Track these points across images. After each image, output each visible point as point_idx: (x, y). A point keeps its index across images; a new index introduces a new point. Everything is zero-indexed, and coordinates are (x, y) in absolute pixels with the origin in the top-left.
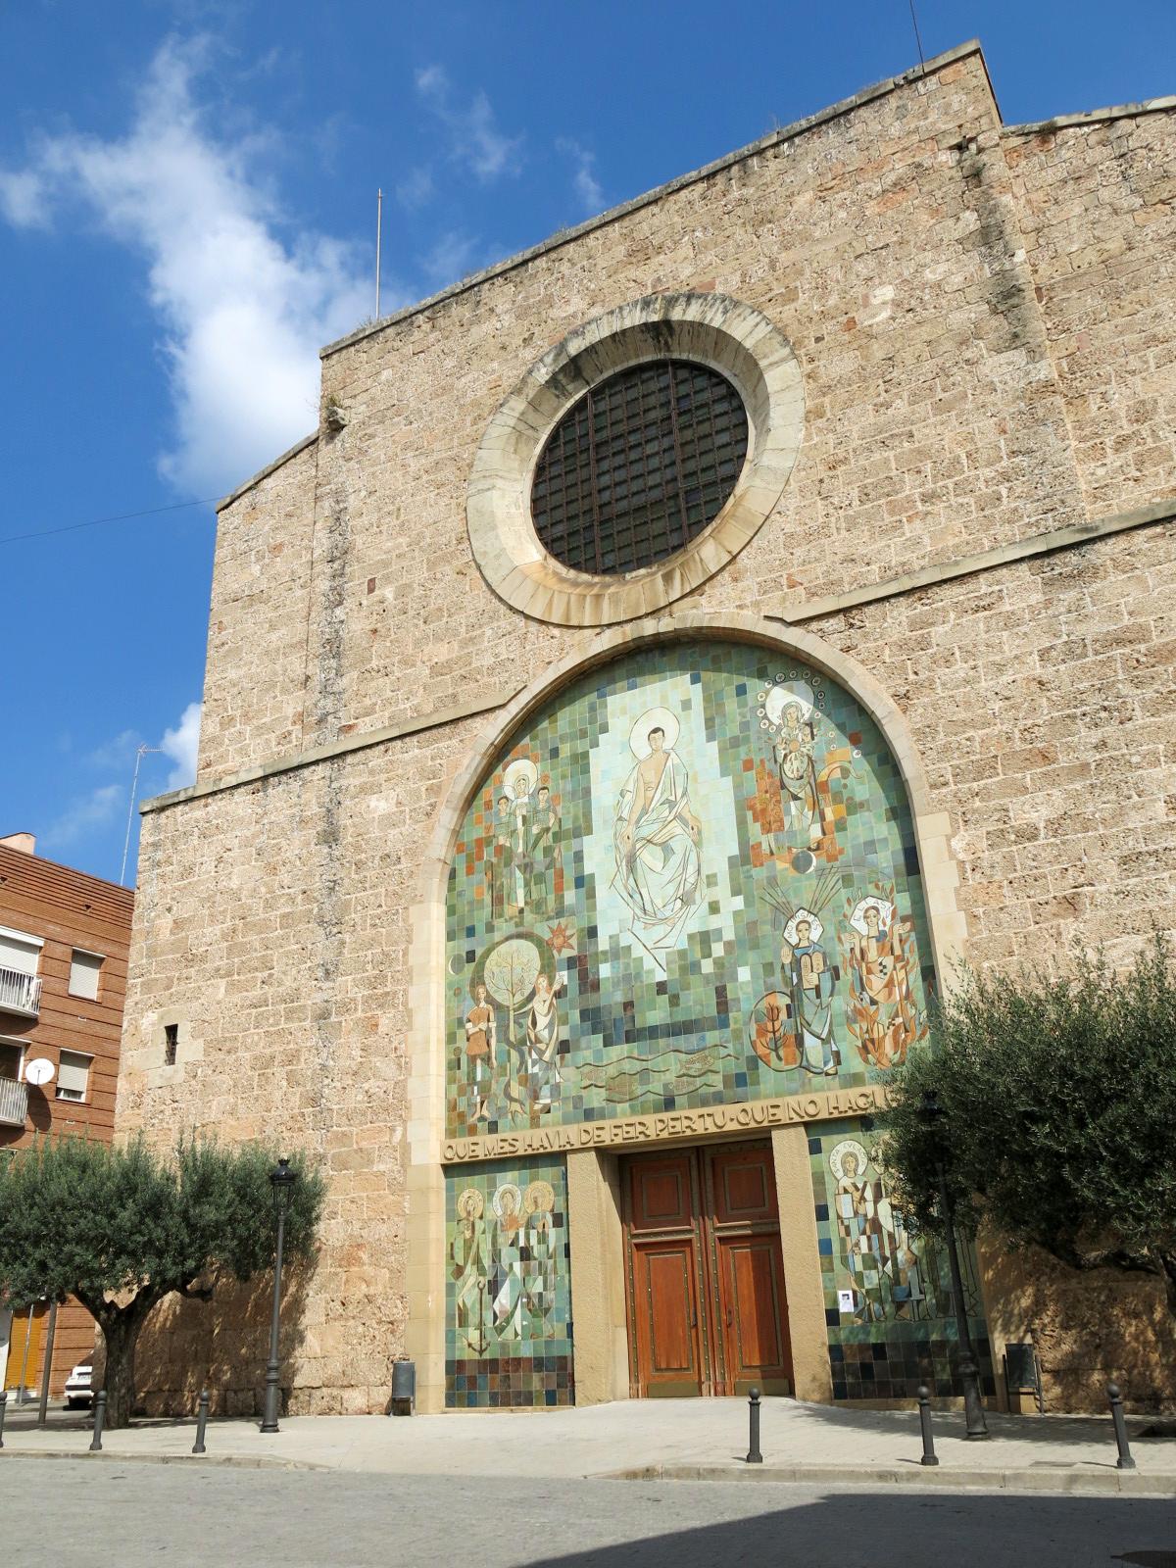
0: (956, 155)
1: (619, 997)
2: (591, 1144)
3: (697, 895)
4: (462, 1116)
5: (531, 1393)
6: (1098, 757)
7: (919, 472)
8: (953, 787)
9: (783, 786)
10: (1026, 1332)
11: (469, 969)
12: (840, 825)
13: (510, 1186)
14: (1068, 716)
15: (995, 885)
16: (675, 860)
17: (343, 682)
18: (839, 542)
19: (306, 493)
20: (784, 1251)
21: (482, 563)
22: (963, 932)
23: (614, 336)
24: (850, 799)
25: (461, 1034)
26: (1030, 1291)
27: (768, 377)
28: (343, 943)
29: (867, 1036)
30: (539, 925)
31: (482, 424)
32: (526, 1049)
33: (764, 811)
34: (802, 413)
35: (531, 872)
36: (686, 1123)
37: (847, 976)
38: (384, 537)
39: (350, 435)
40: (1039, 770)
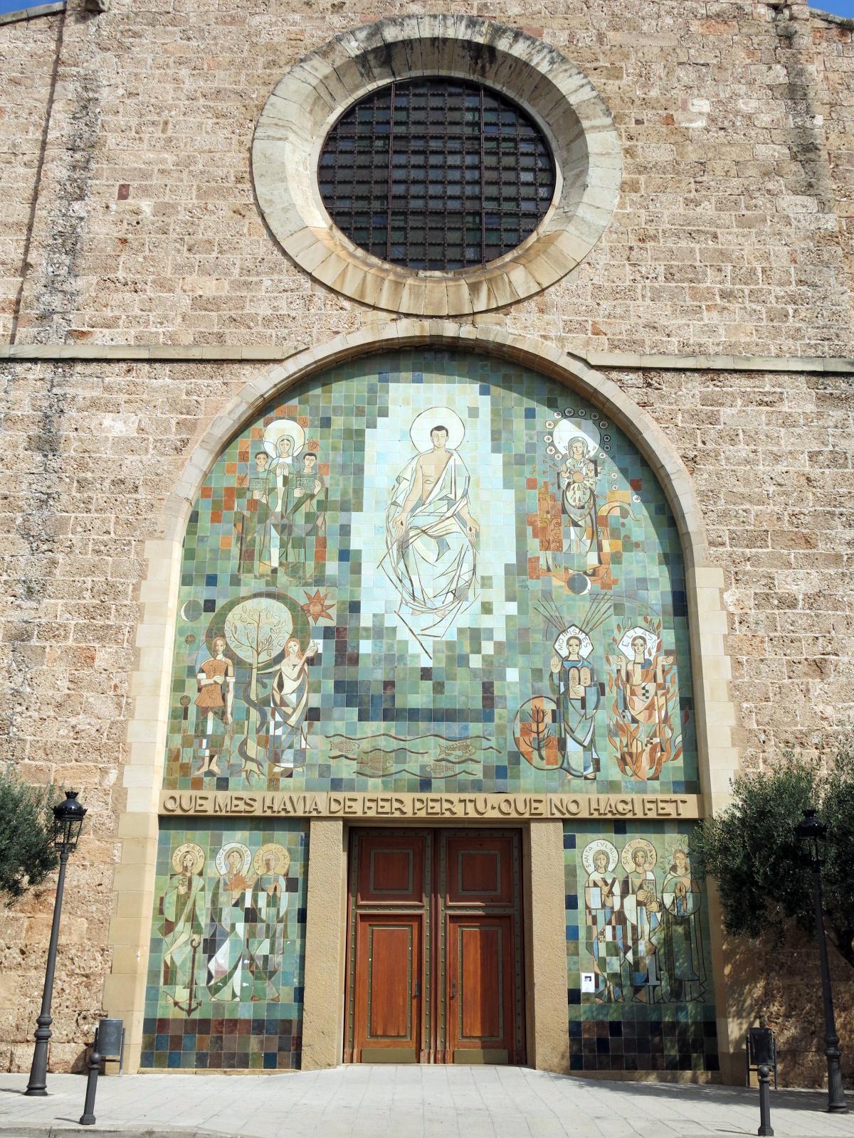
0: (771, 13)
1: (380, 675)
2: (341, 814)
4: (185, 769)
5: (247, 1055)
6: (849, 552)
7: (719, 270)
8: (729, 548)
9: (564, 511)
10: (756, 1018)
11: (206, 619)
12: (616, 559)
13: (239, 846)
14: (829, 512)
15: (758, 639)
16: (450, 556)
17: (80, 283)
18: (643, 308)
19: (40, 65)
20: (534, 933)
21: (267, 210)
22: (727, 674)
23: (434, 40)
24: (627, 537)
25: (191, 684)
26: (761, 984)
27: (590, 137)
28: (54, 563)
29: (626, 749)
30: (294, 588)
31: (276, 71)
32: (268, 710)
33: (544, 529)
34: (618, 182)
35: (290, 534)
36: (446, 805)
37: (612, 694)
38: (145, 146)
39: (109, 23)
40: (801, 551)
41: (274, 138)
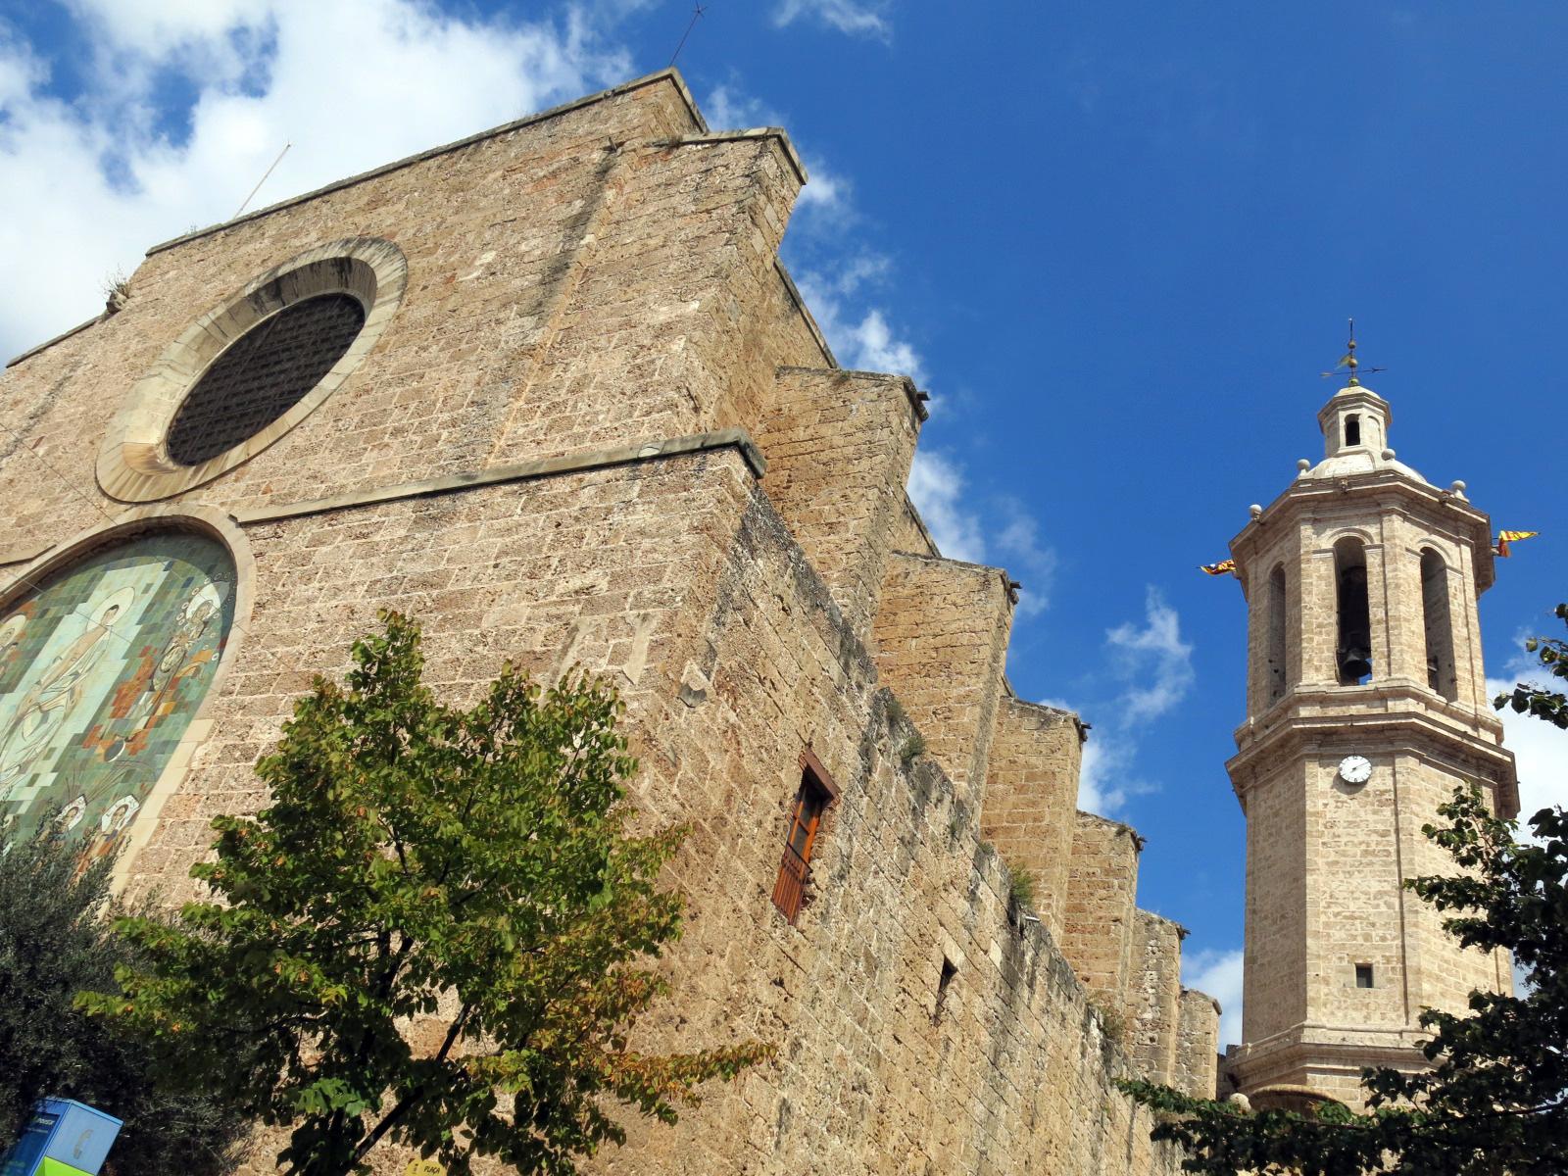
23: (312, 265)
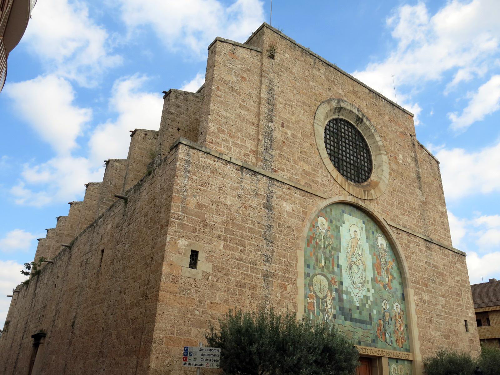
3: (365, 285)
28: (273, 251)
36: (367, 351)
41: (319, 125)
